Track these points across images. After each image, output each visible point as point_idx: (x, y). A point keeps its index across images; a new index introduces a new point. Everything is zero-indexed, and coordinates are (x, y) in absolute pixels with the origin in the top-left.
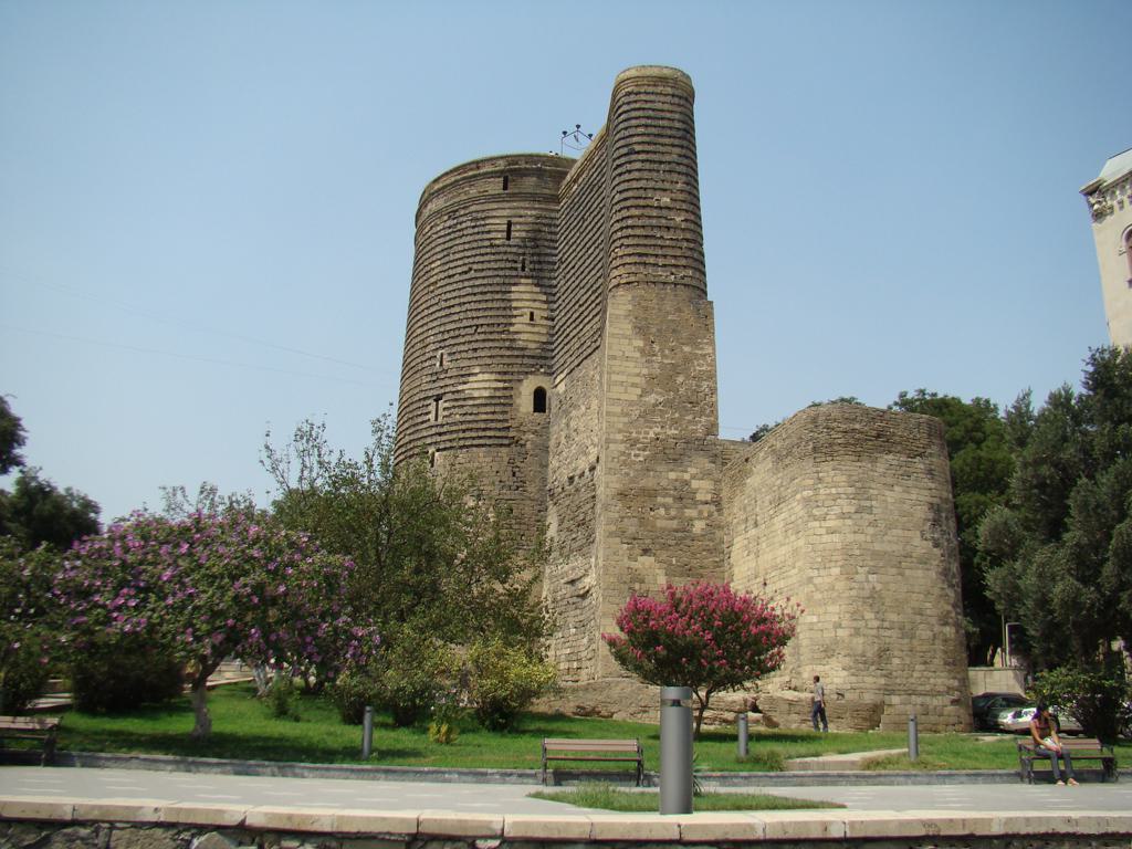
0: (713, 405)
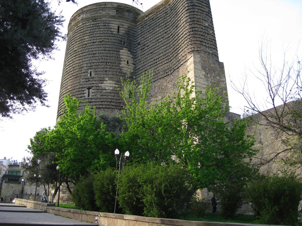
0: (227, 99)
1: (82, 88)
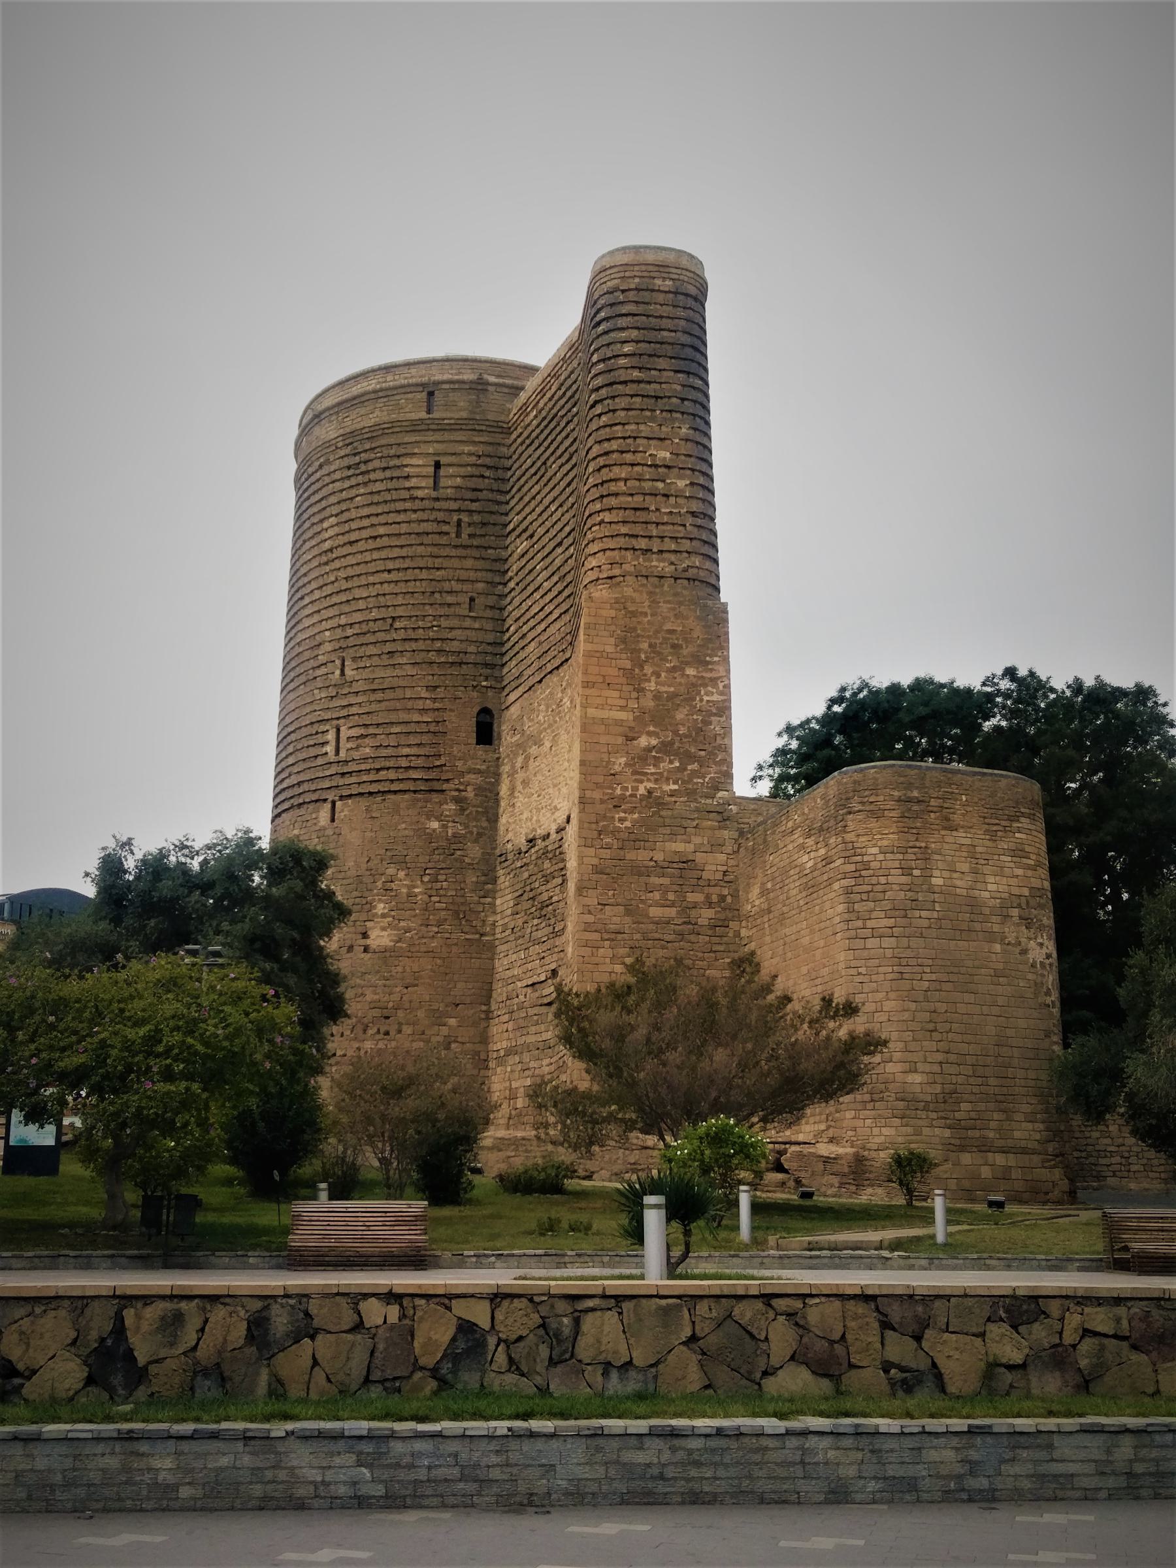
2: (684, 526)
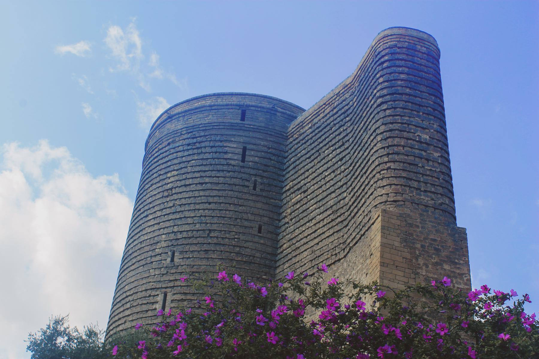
1: (151, 289)
2: (439, 179)
